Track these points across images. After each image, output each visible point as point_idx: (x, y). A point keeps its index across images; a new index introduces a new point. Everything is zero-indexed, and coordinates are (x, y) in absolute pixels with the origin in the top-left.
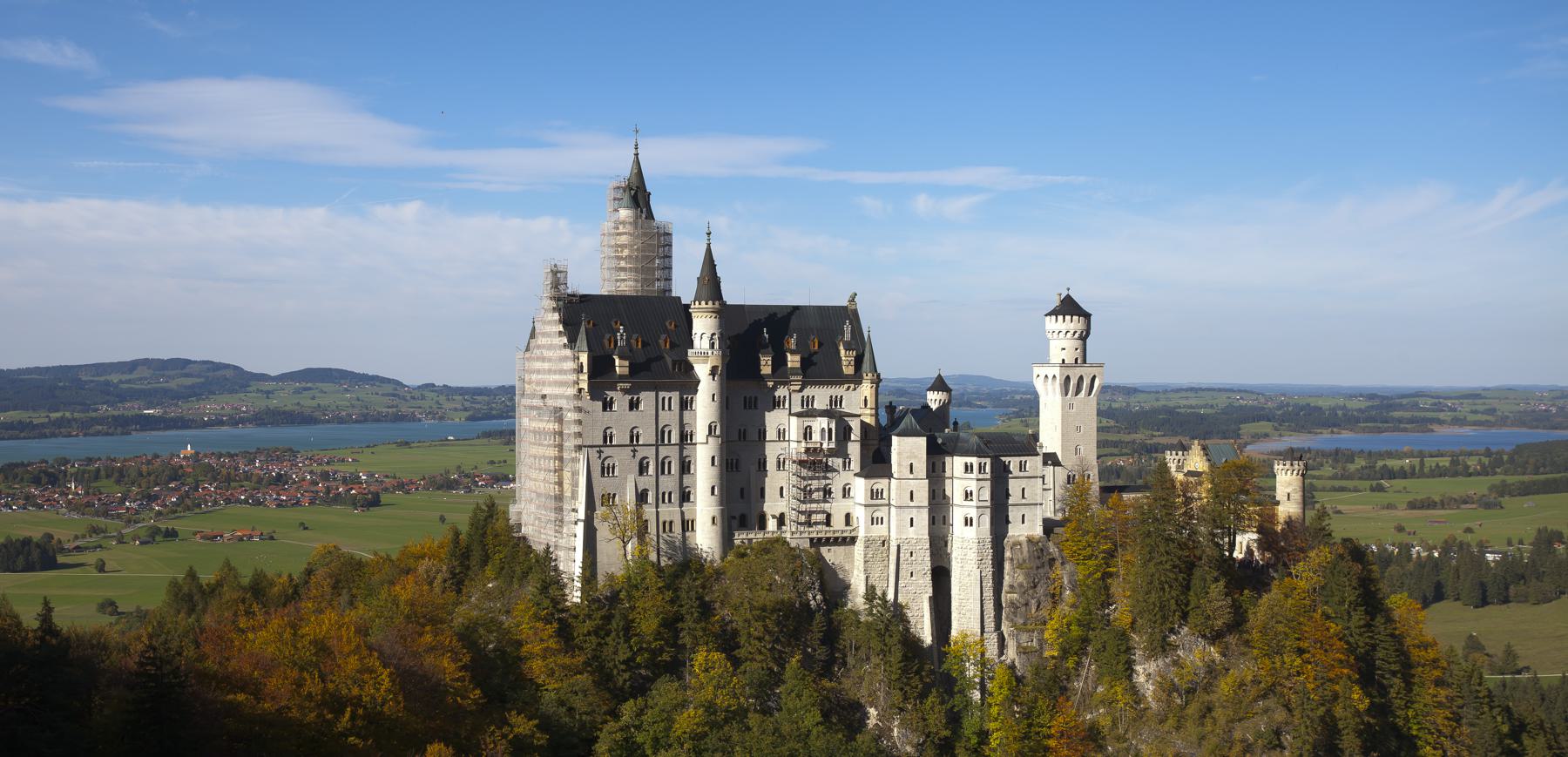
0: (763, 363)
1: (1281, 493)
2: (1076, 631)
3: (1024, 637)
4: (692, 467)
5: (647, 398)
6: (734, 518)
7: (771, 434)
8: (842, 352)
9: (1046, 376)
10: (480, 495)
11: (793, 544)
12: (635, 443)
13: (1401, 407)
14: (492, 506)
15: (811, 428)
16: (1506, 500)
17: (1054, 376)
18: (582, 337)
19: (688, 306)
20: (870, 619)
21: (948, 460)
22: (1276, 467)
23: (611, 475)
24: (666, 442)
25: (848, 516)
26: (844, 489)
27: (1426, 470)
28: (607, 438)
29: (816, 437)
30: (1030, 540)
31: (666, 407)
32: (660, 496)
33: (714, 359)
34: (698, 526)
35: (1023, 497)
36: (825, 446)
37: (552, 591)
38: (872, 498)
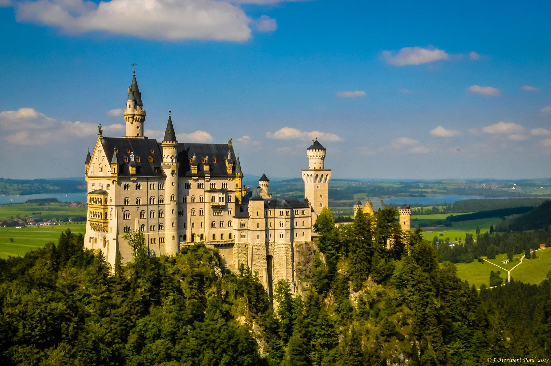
0: (192, 169)
1: (401, 222)
2: (326, 281)
3: (305, 284)
4: (163, 214)
5: (143, 184)
6: (181, 236)
7: (197, 200)
8: (227, 164)
9: (308, 175)
10: (61, 228)
11: (207, 247)
12: (138, 204)
13: (413, 187)
14: (69, 233)
15: (214, 197)
16: (453, 223)
17: (311, 175)
18: (114, 158)
19: (161, 144)
20: (241, 278)
21: (272, 210)
22: (400, 211)
23: (128, 218)
24: (152, 204)
25: (230, 235)
26: (229, 223)
27: (424, 211)
28: (126, 202)
29: (217, 200)
30: (306, 243)
31: (152, 188)
32: (149, 227)
33: (174, 167)
34: (166, 241)
35: (303, 225)
36: (220, 204)
37: (104, 271)
38: (241, 227)
